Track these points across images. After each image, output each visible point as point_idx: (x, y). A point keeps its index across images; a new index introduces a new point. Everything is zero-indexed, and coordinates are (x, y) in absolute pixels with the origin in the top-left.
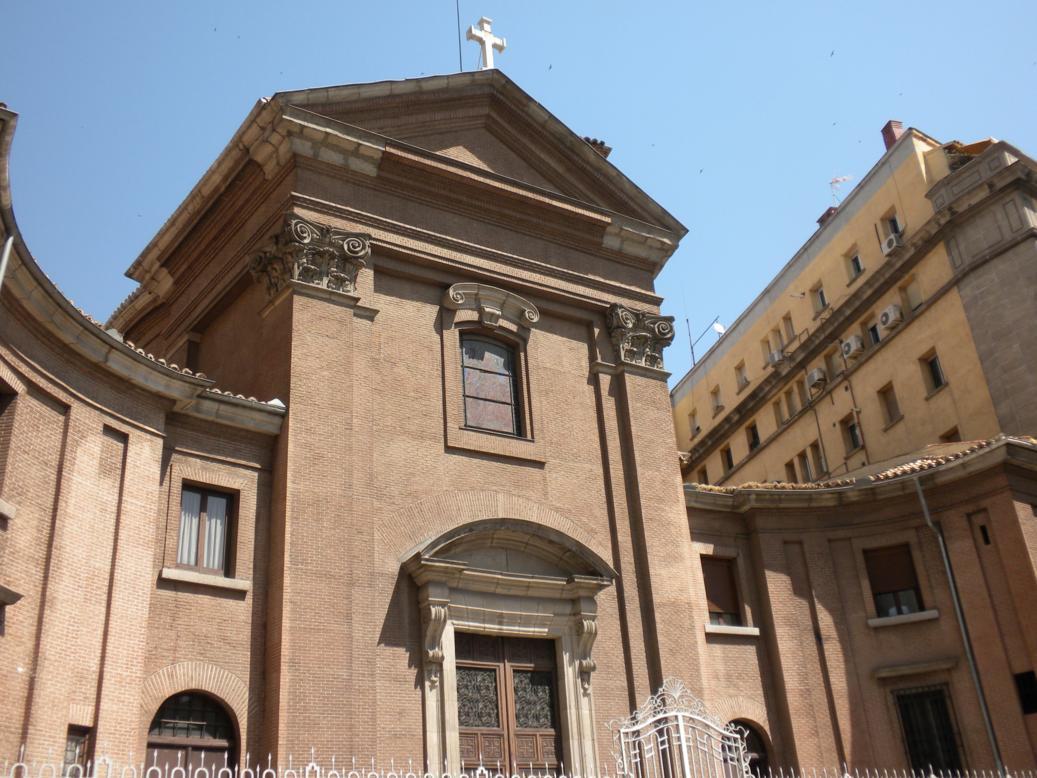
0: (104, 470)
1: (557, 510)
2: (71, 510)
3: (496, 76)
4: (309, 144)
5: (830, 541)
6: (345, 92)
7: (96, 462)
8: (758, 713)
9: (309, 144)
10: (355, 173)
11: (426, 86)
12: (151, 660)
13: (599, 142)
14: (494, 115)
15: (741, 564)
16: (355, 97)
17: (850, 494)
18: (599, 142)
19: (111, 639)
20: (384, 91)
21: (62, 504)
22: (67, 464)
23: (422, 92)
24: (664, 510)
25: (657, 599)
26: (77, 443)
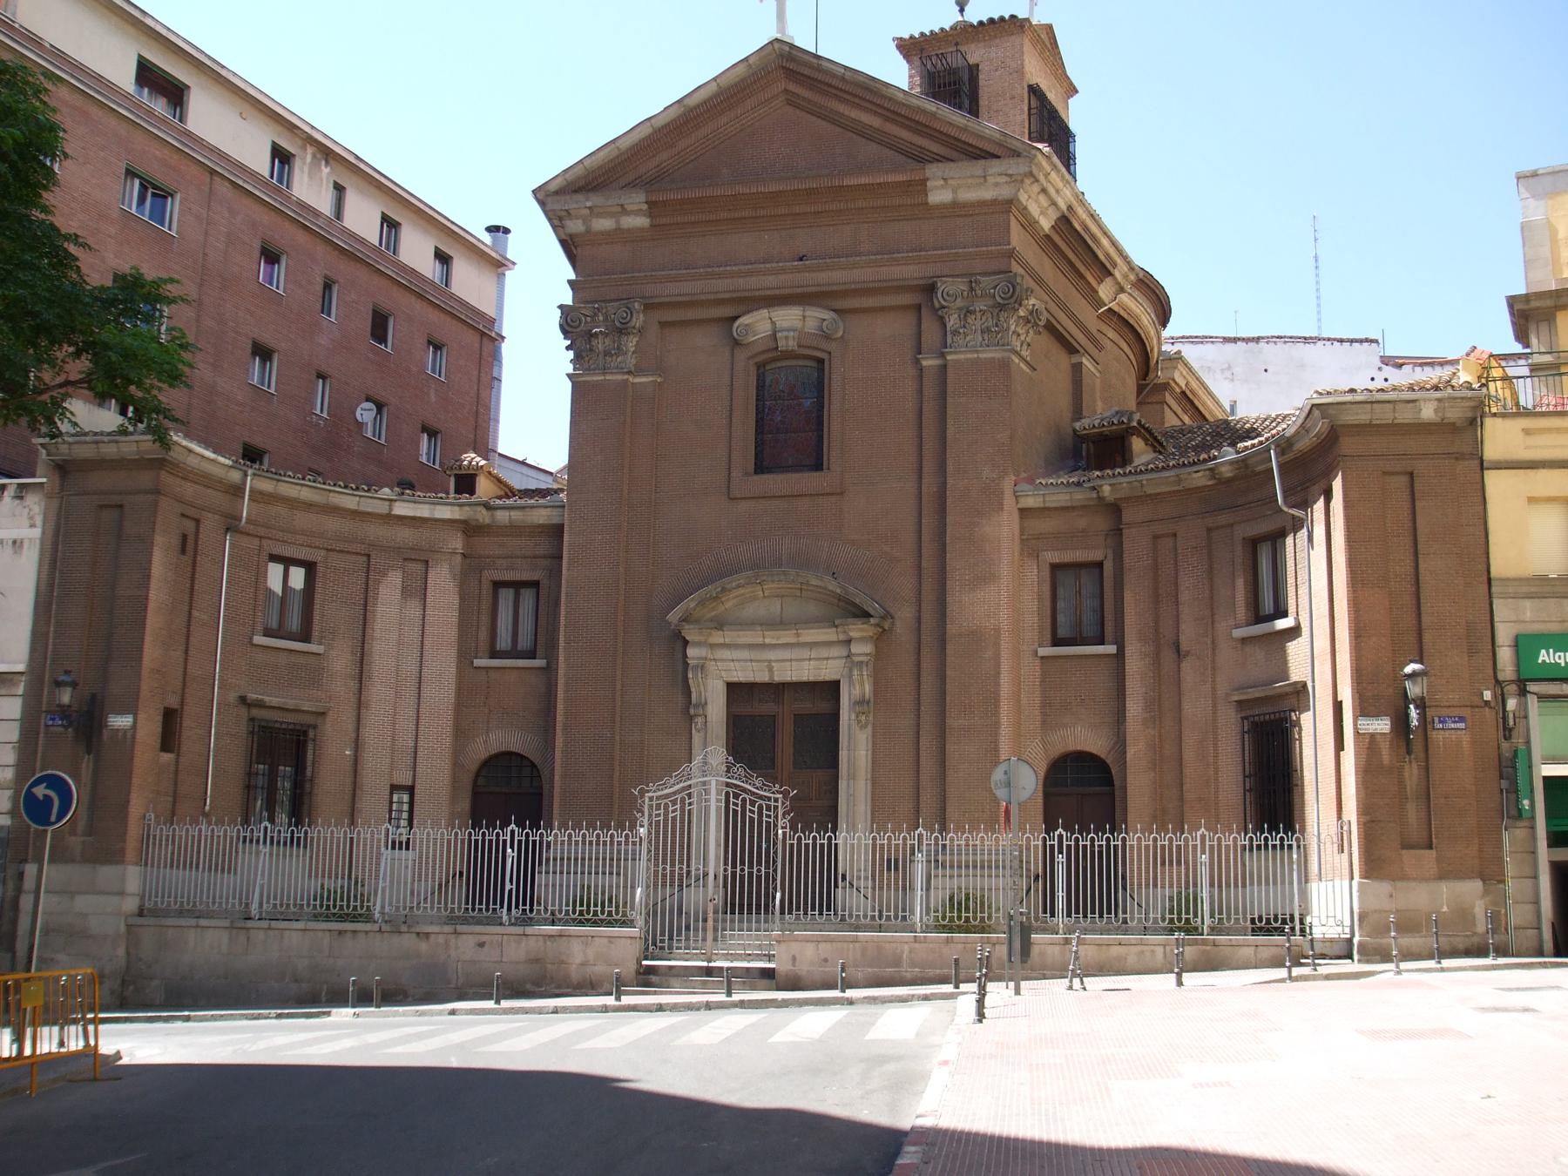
0: (406, 592)
2: (377, 634)
3: (776, 46)
4: (580, 222)
5: (1209, 530)
6: (602, 154)
7: (398, 592)
8: (1088, 738)
9: (580, 222)
10: (629, 230)
11: (692, 102)
12: (461, 733)
13: (1007, 17)
14: (792, 87)
15: (1108, 567)
16: (616, 153)
17: (1224, 469)
18: (1007, 17)
19: (422, 722)
20: (647, 130)
21: (369, 631)
22: (370, 600)
25: (951, 629)
26: (378, 582)
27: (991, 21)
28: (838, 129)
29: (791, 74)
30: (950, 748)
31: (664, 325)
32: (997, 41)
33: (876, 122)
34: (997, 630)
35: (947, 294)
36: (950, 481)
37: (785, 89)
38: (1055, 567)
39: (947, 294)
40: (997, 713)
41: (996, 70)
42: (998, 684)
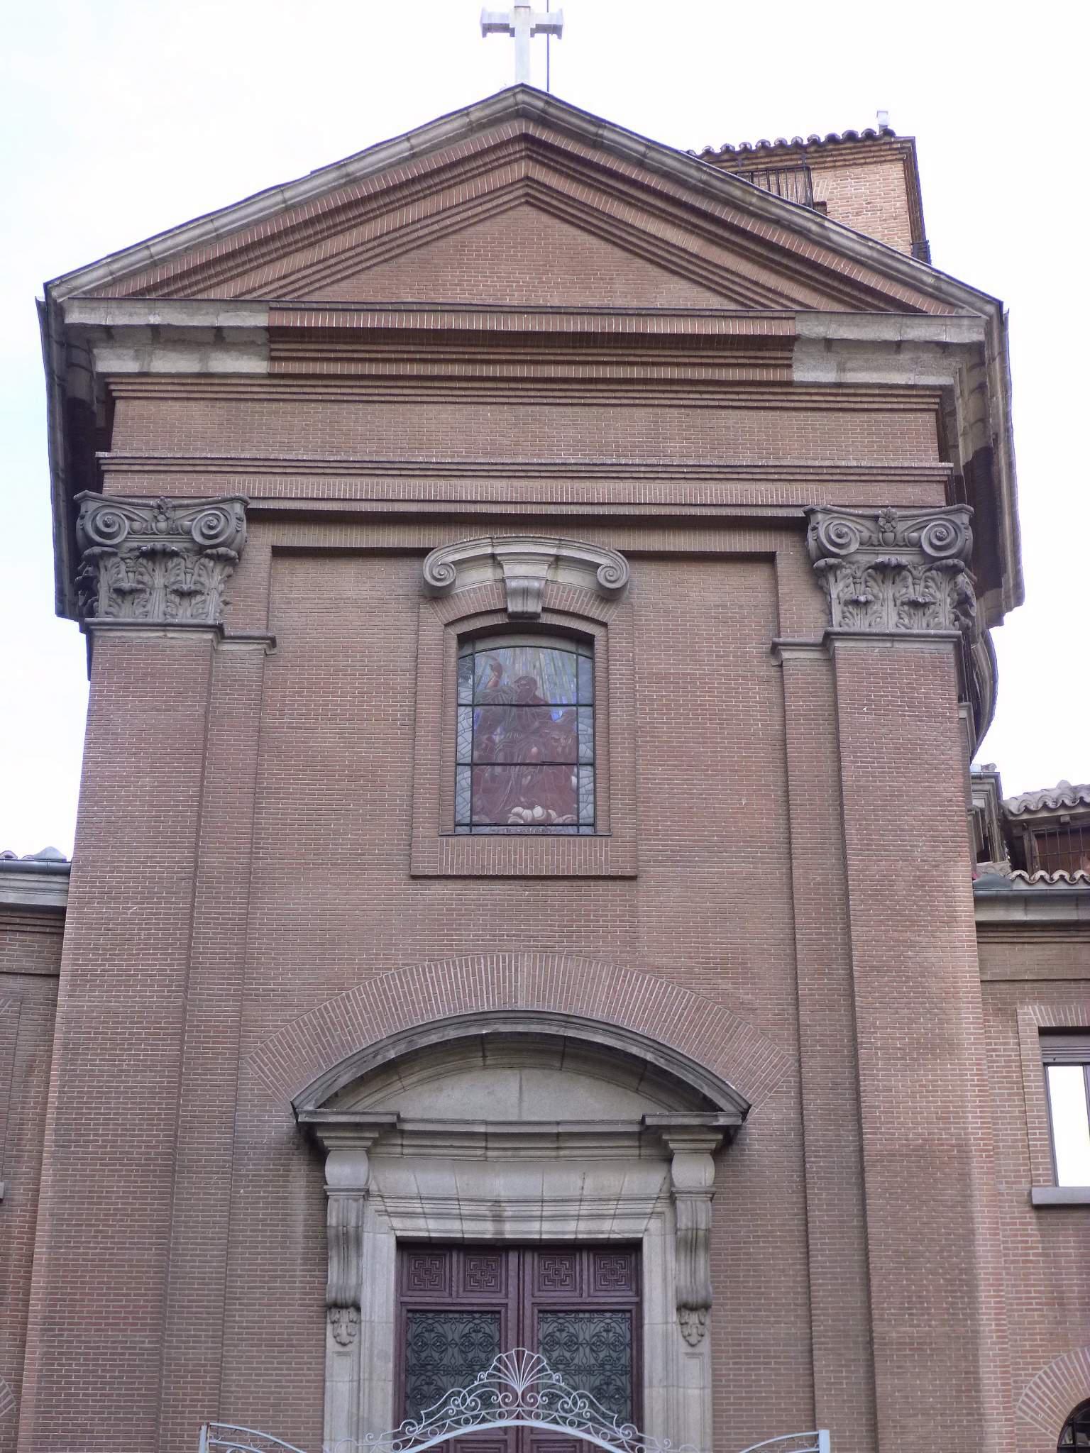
1: (657, 971)
14: (540, 174)
23: (353, 180)
24: (912, 945)
25: (874, 1143)
27: (851, 136)
28: (619, 253)
29: (537, 149)
30: (884, 1383)
31: (279, 552)
32: (857, 170)
33: (693, 244)
34: (963, 1149)
35: (840, 536)
36: (854, 862)
37: (527, 178)
38: (1044, 1032)
39: (840, 536)
40: (973, 1314)
41: (858, 214)
42: (971, 1256)
